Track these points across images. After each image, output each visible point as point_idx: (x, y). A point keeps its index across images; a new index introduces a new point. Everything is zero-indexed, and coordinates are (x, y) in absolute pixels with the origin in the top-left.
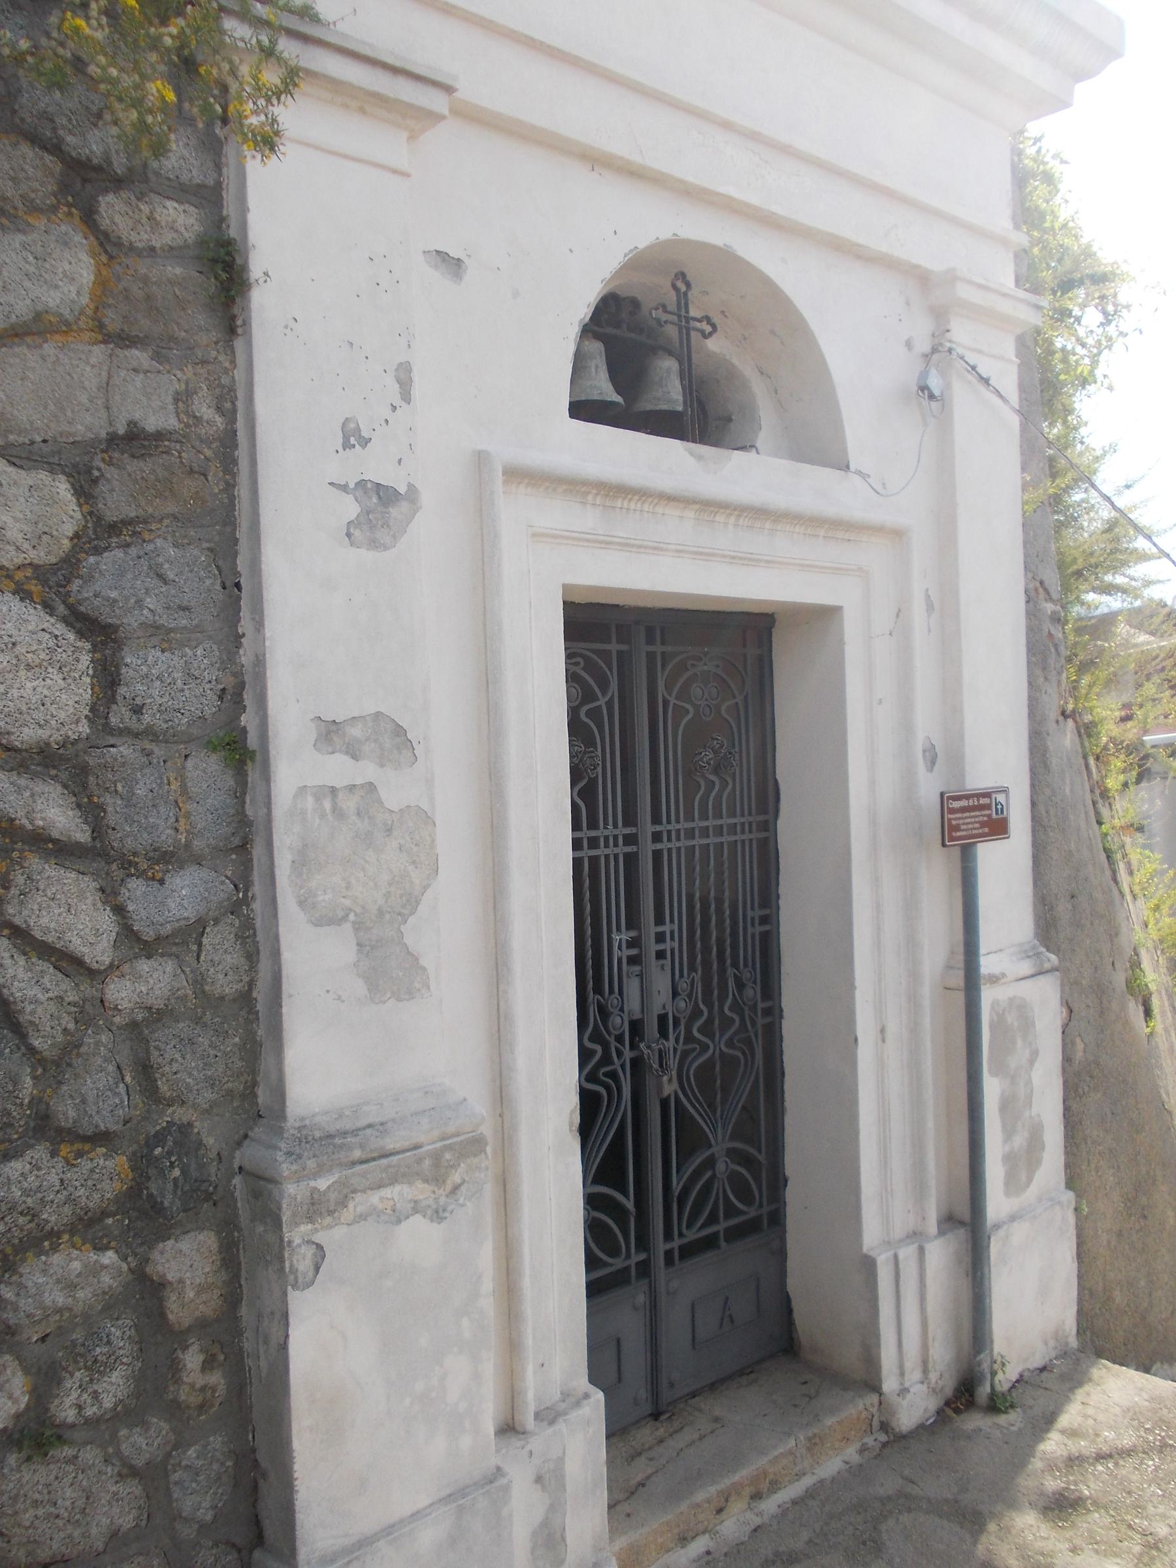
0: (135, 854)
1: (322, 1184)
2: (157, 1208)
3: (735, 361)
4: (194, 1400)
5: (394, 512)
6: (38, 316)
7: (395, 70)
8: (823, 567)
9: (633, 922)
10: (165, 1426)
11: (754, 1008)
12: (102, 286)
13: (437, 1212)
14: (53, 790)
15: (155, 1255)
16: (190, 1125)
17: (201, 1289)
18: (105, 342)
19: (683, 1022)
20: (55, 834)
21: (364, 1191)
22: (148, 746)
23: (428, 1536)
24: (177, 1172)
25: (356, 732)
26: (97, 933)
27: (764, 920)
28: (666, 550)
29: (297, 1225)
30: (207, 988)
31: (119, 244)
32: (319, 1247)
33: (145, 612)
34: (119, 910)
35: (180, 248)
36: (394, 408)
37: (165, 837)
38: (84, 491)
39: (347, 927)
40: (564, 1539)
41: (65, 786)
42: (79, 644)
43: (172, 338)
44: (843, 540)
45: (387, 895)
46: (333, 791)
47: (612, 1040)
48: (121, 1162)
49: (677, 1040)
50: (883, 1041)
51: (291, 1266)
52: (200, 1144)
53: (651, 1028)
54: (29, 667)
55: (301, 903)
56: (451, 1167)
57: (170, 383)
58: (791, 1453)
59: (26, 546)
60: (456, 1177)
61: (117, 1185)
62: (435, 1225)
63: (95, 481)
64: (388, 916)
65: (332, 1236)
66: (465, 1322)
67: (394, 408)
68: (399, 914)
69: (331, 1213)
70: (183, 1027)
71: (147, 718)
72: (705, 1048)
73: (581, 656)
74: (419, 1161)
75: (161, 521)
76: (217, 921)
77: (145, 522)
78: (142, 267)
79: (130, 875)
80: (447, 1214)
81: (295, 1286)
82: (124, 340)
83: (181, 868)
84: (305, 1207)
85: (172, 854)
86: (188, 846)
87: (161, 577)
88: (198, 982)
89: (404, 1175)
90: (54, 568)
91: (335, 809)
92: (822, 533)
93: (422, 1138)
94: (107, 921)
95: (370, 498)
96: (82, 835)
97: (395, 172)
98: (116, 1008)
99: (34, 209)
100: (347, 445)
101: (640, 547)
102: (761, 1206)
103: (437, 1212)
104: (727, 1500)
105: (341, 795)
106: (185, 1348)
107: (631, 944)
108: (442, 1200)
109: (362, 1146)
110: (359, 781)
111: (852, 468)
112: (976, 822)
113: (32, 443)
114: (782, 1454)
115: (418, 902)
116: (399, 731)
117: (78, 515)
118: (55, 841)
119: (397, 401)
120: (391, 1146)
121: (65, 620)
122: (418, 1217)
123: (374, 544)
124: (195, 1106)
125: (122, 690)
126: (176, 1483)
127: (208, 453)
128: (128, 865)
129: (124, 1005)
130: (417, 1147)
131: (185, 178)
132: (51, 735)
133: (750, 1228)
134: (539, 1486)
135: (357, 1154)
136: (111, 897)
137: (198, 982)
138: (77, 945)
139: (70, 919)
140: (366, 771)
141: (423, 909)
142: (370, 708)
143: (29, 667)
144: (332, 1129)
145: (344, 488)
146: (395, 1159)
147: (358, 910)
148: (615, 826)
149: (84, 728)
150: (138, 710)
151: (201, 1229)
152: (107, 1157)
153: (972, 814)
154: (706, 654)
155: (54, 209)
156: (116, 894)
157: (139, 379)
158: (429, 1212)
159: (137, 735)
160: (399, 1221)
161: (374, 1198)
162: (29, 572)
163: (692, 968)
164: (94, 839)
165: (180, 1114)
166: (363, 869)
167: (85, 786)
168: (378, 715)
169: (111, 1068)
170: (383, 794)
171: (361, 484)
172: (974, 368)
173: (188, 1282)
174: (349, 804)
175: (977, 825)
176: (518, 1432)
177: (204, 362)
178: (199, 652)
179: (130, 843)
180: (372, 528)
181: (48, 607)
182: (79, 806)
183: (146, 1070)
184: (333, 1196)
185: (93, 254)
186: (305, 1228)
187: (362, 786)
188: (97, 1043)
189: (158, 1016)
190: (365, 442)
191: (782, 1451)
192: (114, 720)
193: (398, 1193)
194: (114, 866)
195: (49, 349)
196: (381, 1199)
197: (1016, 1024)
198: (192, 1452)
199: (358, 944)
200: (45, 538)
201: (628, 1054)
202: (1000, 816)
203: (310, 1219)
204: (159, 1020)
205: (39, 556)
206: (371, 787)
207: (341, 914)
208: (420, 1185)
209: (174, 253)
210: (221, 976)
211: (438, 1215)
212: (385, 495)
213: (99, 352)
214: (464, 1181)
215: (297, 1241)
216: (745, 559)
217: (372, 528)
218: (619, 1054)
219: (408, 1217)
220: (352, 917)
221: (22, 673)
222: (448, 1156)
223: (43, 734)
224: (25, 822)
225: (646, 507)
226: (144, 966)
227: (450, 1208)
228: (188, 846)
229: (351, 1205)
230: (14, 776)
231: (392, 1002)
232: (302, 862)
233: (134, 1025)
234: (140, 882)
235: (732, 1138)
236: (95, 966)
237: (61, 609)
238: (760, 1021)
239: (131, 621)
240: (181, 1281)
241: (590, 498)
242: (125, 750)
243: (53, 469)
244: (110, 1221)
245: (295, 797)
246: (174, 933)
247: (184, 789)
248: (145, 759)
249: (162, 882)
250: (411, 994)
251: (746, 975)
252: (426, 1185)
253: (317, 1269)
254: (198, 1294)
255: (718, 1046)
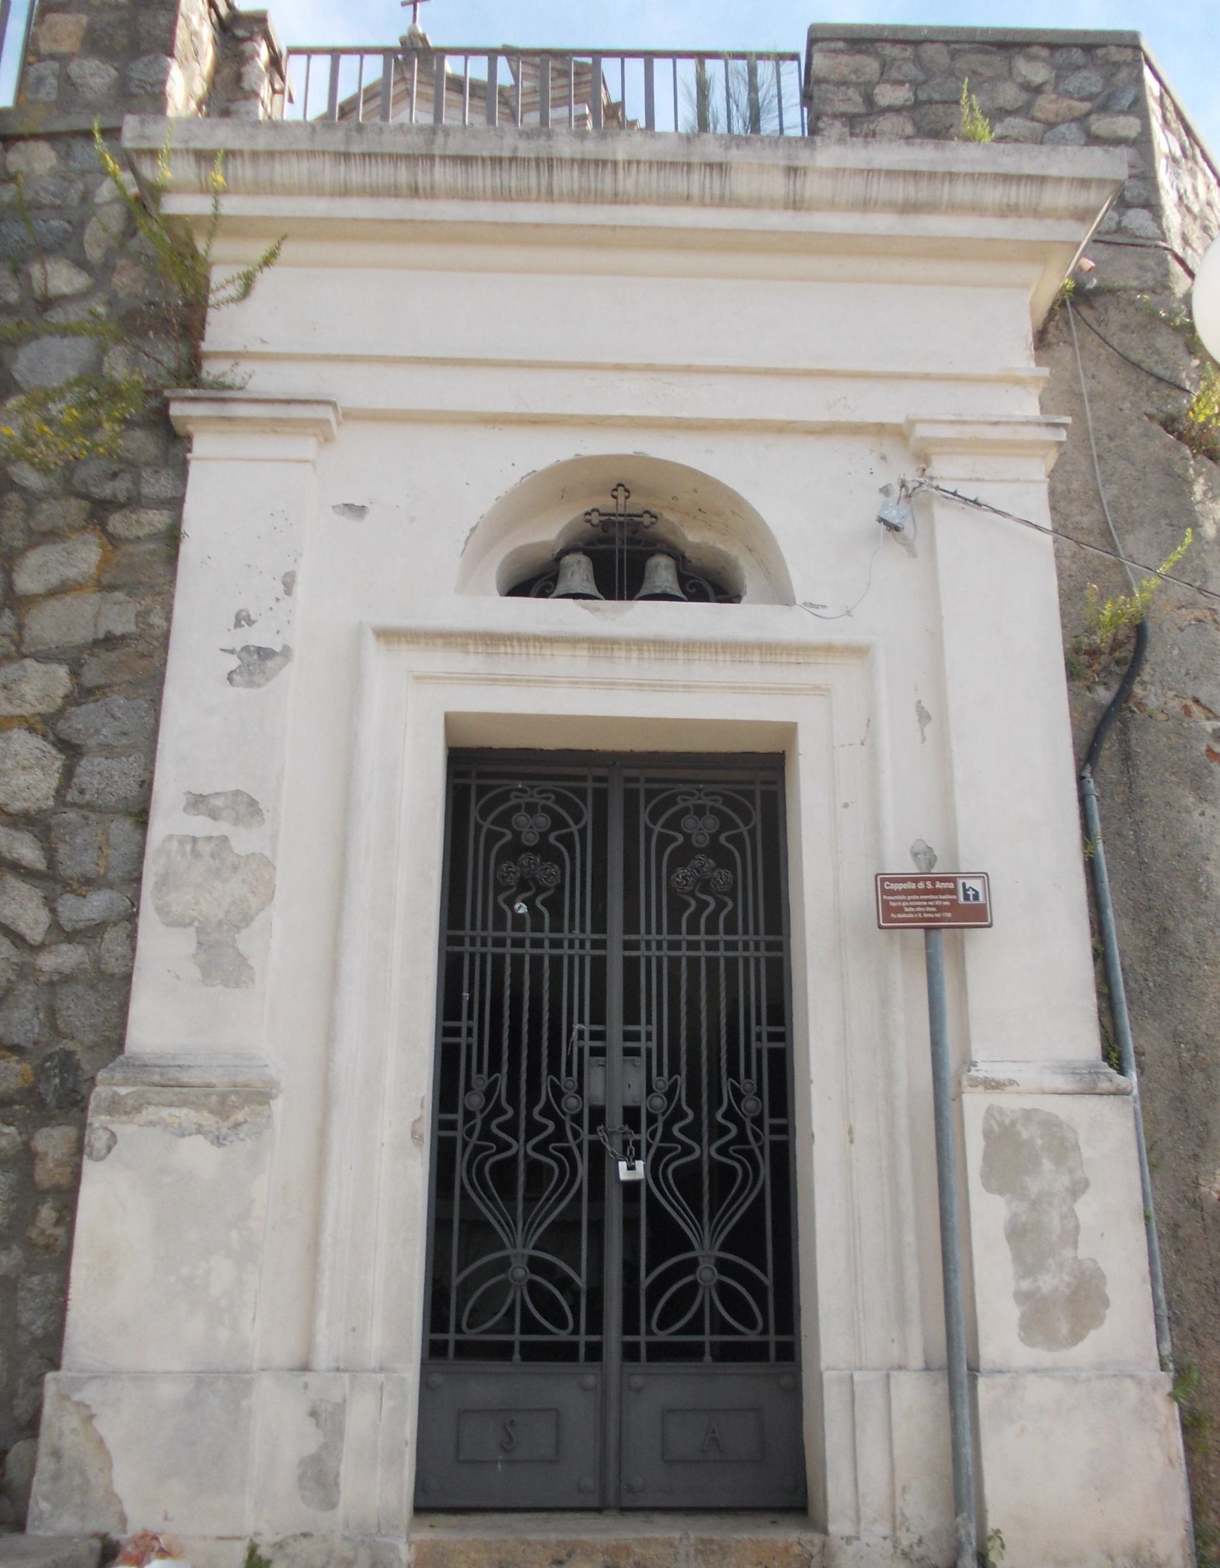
0: (72, 879)
1: (123, 1091)
2: (42, 1104)
3: (721, 547)
4: (41, 1241)
5: (269, 663)
6: (63, 583)
7: (289, 402)
8: (770, 689)
9: (599, 1016)
10: (19, 1252)
11: (758, 1121)
12: (104, 562)
13: (218, 1138)
14: (27, 837)
15: (37, 1136)
16: (74, 1053)
17: (59, 1163)
18: (100, 591)
19: (661, 1120)
20: (24, 863)
21: (157, 1105)
22: (86, 813)
23: (167, 1392)
24: (57, 1081)
25: (219, 802)
26: (37, 922)
27: (781, 1037)
28: (557, 682)
29: (99, 1114)
30: (102, 966)
31: (119, 539)
32: (113, 1134)
33: (101, 737)
34: (53, 911)
35: (156, 534)
36: (278, 600)
37: (89, 869)
38: (74, 674)
39: (192, 930)
40: (337, 1485)
41: (35, 836)
42: (59, 756)
43: (140, 583)
44: (788, 663)
45: (228, 912)
46: (194, 840)
47: (567, 1120)
48: (26, 1068)
49: (653, 1135)
50: (852, 1142)
51: (89, 1142)
52: (78, 1067)
53: (615, 1119)
54: (24, 768)
55: (159, 910)
56: (237, 1107)
57: (133, 608)
58: (670, 1544)
59: (36, 703)
60: (239, 1116)
61: (20, 1081)
62: (215, 1147)
63: (82, 666)
64: (225, 927)
65: (126, 1130)
66: (234, 1235)
67: (278, 600)
68: (236, 927)
69: (126, 1113)
70: (80, 989)
71: (88, 797)
72: (688, 1150)
73: (553, 792)
74: (207, 1095)
75: (120, 685)
76: (115, 924)
77: (110, 686)
78: (129, 548)
79: (67, 892)
80: (225, 1142)
81: (90, 1156)
82: (112, 588)
83: (99, 889)
84: (107, 1103)
85: (94, 880)
86: (105, 876)
87: (113, 716)
88: (97, 962)
89: (193, 1103)
90: (52, 716)
91: (193, 851)
92: (756, 658)
93: (214, 1081)
94: (44, 917)
95: (252, 656)
96: (41, 866)
97: (299, 461)
98: (40, 971)
99: (74, 529)
100: (238, 624)
101: (528, 681)
102: (765, 1331)
103: (218, 1138)
104: (569, 1555)
105: (200, 843)
106: (44, 1203)
107: (595, 1036)
108: (224, 1131)
109: (162, 1074)
110: (215, 834)
111: (799, 601)
112: (934, 906)
113: (50, 649)
114: (656, 1539)
115: (252, 919)
116: (253, 803)
117: (69, 685)
118: (25, 868)
119: (281, 594)
120: (186, 1080)
121: (53, 744)
122: (200, 1138)
123: (251, 684)
124: (82, 1043)
125: (76, 780)
126: (22, 1298)
127: (156, 644)
128: (67, 886)
129: (45, 969)
130: (209, 1086)
131: (162, 496)
132: (31, 806)
133: (755, 1352)
134: (313, 1421)
135: (156, 1078)
136: (50, 903)
137: (97, 962)
138: (22, 927)
139: (20, 911)
140: (223, 828)
141: (256, 924)
142: (231, 787)
143: (24, 768)
144: (148, 1062)
145: (232, 652)
146: (185, 1090)
147: (202, 919)
148: (583, 930)
149: (51, 803)
150: (82, 792)
151: (68, 1124)
152: (18, 1062)
153: (922, 897)
154: (700, 790)
155: (84, 528)
156: (54, 900)
157: (116, 608)
158: (211, 1136)
159: (81, 807)
160: (183, 1135)
161: (165, 1113)
162: (38, 718)
163: (674, 1069)
164: (48, 868)
165: (68, 1045)
166: (210, 893)
167: (48, 838)
168: (237, 793)
169: (31, 1007)
170: (234, 843)
171: (246, 649)
172: (955, 494)
173: (50, 1155)
174: (205, 849)
175: (934, 909)
176: (310, 1370)
177: (159, 594)
178: (131, 759)
179: (69, 872)
180: (251, 674)
181: (45, 737)
182: (43, 849)
183: (52, 1012)
184: (130, 1102)
185: (102, 546)
186: (103, 1117)
187: (217, 838)
188: (27, 990)
189: (67, 979)
190: (250, 622)
191: (657, 1536)
192: (69, 798)
193: (185, 1115)
194: (59, 886)
195: (68, 599)
196: (170, 1115)
197: (1039, 1142)
198: (36, 1279)
199: (199, 943)
200: (47, 698)
201: (586, 1136)
202: (972, 902)
203: (110, 1113)
204: (66, 982)
205: (42, 708)
206: (225, 839)
207: (187, 921)
208: (205, 1114)
209: (151, 537)
210: (113, 960)
211: (218, 1141)
212: (264, 654)
213: (95, 597)
214: (246, 1122)
215: (96, 1125)
216: (655, 685)
217: (251, 674)
218: (576, 1135)
219: (190, 1134)
220: (196, 923)
221: (19, 771)
222: (233, 1098)
223: (26, 805)
224: (7, 855)
225: (532, 651)
226: (64, 947)
227: (230, 1138)
228: (105, 876)
229: (144, 1113)
230: (6, 830)
231: (221, 987)
232: (163, 883)
233: (51, 984)
234: (71, 896)
235: (723, 1248)
236: (32, 942)
237: (51, 737)
238: (767, 1138)
239: (92, 743)
240: (46, 1154)
241: (471, 648)
242: (72, 816)
243: (59, 661)
244: (17, 1107)
245: (164, 841)
246: (88, 928)
247: (107, 841)
248: (84, 821)
249: (84, 897)
250: (237, 984)
251: (747, 1086)
252: (211, 1116)
253: (109, 1149)
254: (57, 1166)
255: (706, 1152)
